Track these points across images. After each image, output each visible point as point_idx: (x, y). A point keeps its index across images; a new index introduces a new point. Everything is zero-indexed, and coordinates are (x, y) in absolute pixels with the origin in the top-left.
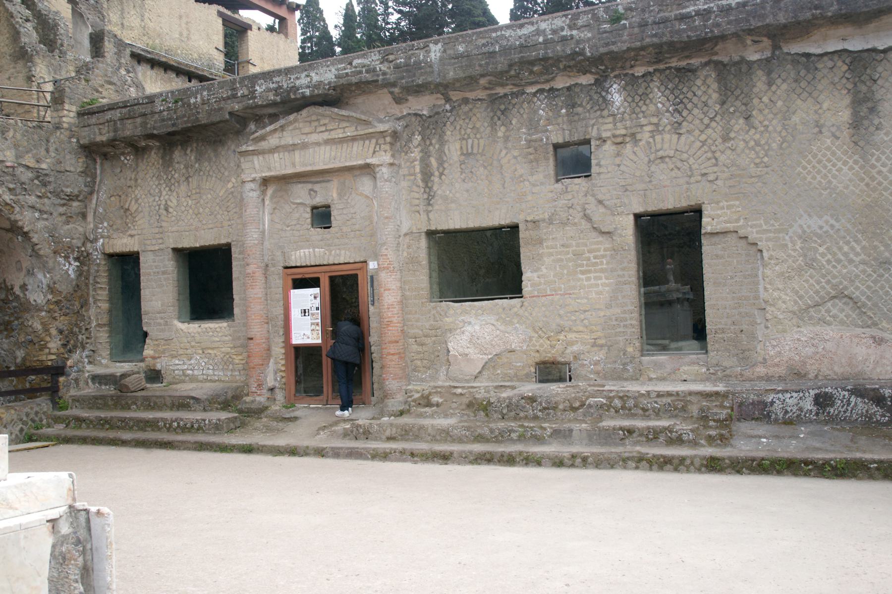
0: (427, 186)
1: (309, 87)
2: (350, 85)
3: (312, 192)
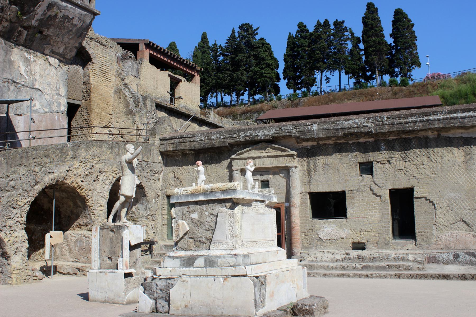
0: (309, 175)
1: (263, 136)
2: (280, 136)
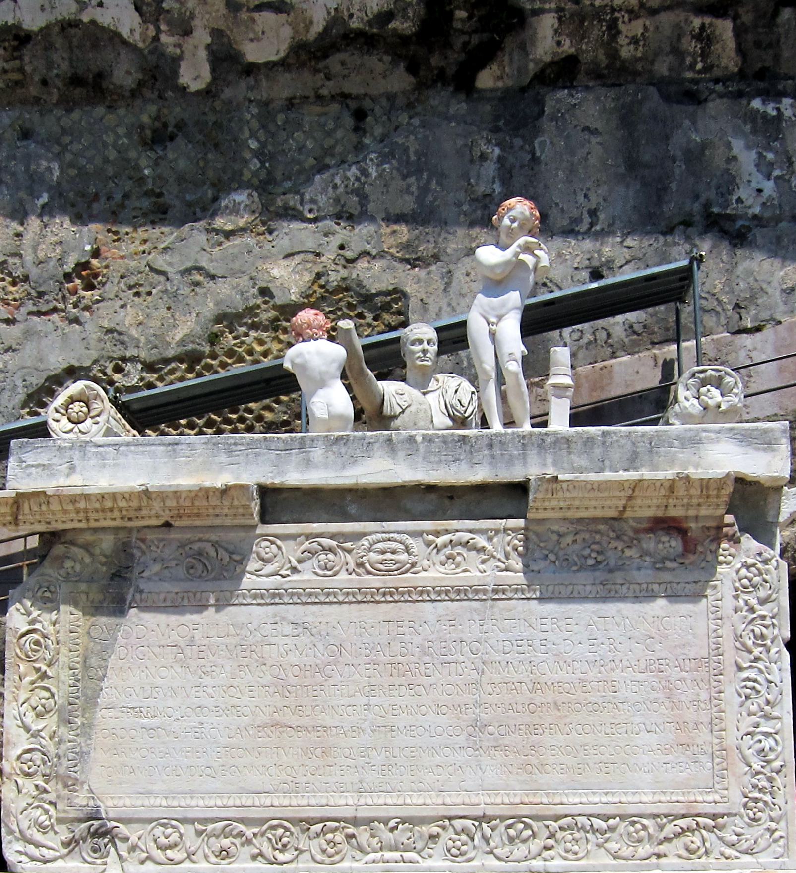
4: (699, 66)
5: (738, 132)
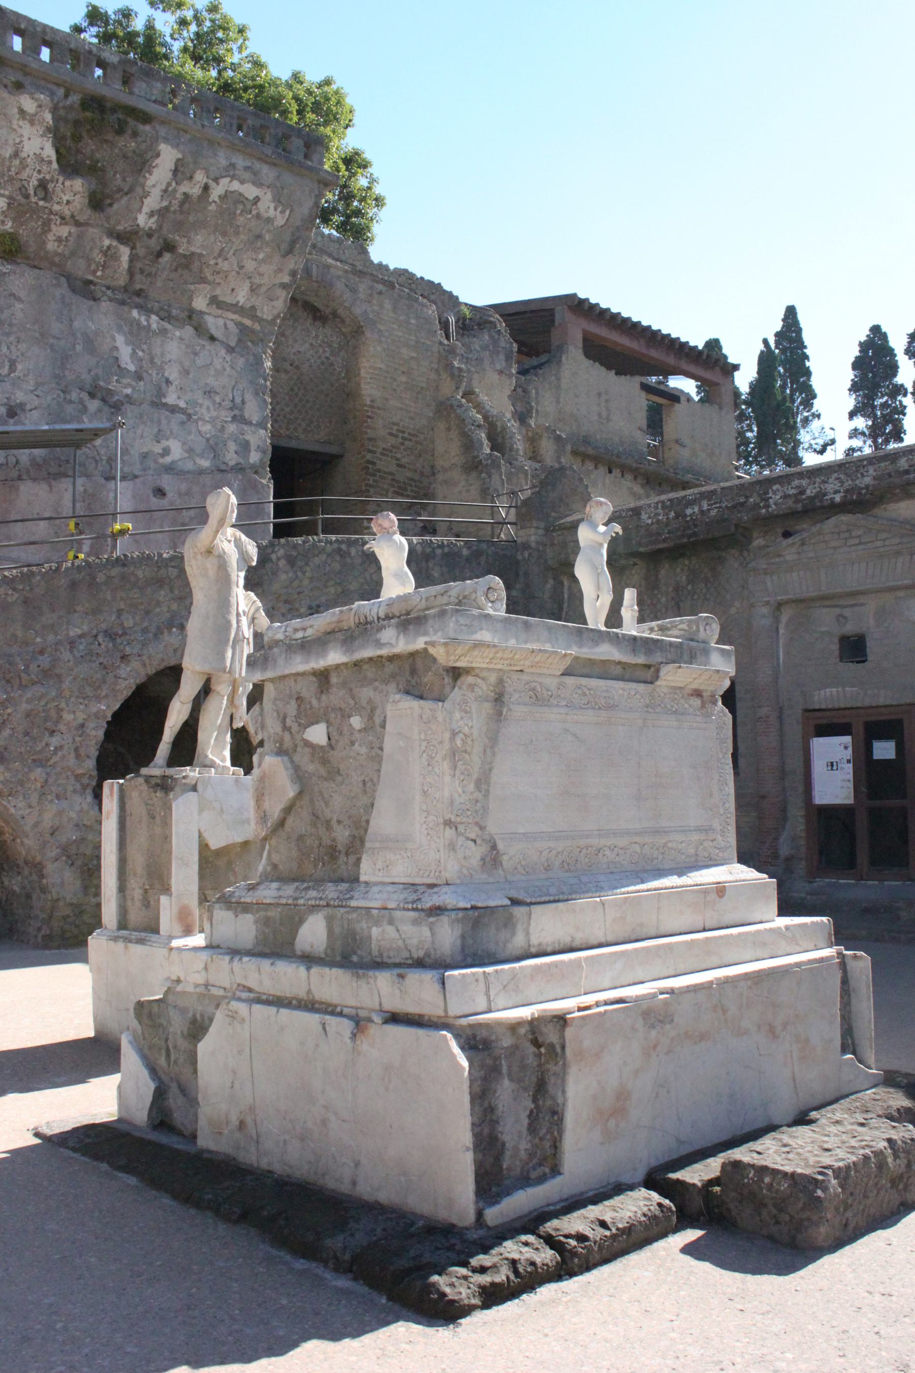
1: (840, 492)
3: (841, 619)
4: (99, 273)
5: (119, 329)
